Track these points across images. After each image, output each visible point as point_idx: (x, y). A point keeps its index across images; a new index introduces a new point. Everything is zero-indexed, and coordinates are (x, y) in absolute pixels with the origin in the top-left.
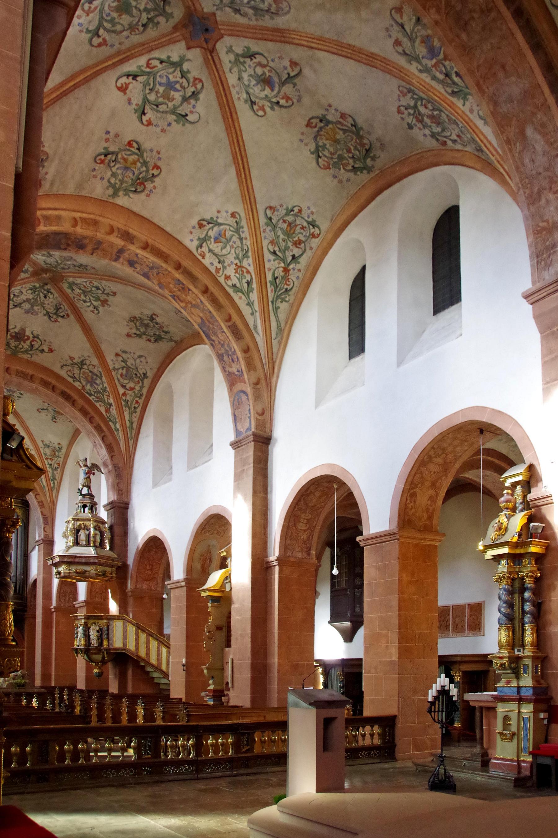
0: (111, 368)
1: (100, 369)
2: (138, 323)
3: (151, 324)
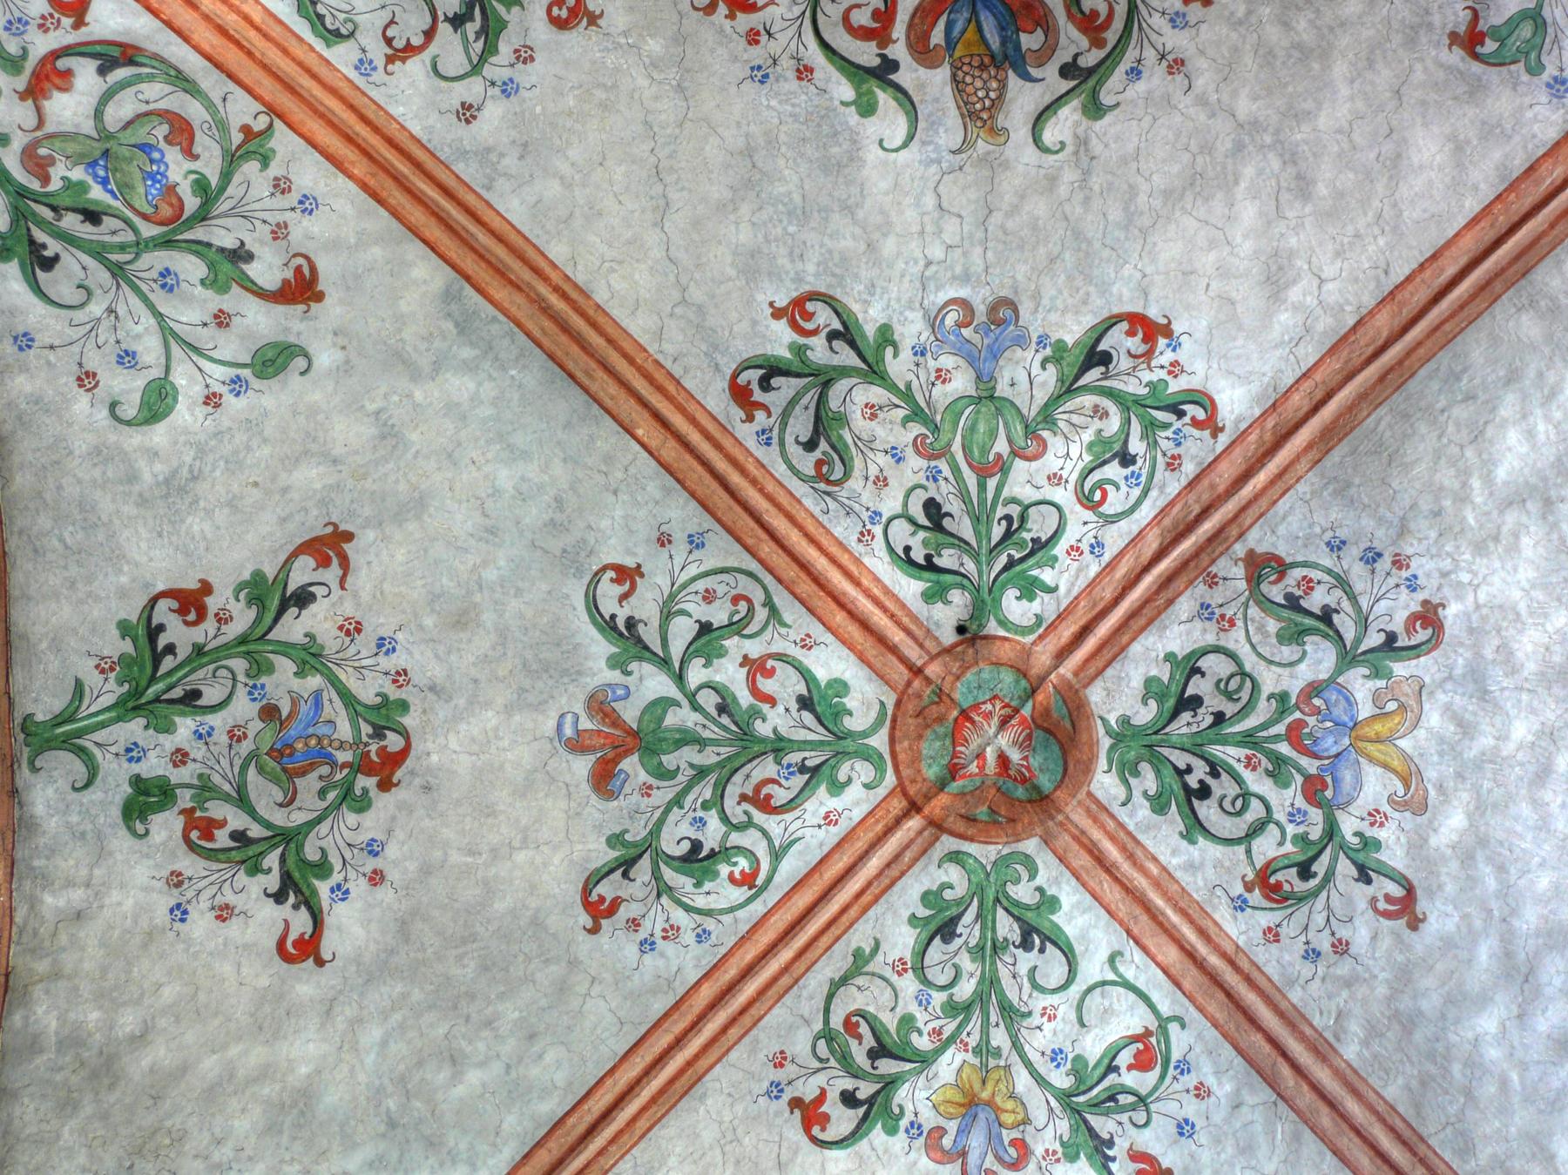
0: (283, 141)
1: (342, 57)
2: (344, 730)
3: (264, 794)
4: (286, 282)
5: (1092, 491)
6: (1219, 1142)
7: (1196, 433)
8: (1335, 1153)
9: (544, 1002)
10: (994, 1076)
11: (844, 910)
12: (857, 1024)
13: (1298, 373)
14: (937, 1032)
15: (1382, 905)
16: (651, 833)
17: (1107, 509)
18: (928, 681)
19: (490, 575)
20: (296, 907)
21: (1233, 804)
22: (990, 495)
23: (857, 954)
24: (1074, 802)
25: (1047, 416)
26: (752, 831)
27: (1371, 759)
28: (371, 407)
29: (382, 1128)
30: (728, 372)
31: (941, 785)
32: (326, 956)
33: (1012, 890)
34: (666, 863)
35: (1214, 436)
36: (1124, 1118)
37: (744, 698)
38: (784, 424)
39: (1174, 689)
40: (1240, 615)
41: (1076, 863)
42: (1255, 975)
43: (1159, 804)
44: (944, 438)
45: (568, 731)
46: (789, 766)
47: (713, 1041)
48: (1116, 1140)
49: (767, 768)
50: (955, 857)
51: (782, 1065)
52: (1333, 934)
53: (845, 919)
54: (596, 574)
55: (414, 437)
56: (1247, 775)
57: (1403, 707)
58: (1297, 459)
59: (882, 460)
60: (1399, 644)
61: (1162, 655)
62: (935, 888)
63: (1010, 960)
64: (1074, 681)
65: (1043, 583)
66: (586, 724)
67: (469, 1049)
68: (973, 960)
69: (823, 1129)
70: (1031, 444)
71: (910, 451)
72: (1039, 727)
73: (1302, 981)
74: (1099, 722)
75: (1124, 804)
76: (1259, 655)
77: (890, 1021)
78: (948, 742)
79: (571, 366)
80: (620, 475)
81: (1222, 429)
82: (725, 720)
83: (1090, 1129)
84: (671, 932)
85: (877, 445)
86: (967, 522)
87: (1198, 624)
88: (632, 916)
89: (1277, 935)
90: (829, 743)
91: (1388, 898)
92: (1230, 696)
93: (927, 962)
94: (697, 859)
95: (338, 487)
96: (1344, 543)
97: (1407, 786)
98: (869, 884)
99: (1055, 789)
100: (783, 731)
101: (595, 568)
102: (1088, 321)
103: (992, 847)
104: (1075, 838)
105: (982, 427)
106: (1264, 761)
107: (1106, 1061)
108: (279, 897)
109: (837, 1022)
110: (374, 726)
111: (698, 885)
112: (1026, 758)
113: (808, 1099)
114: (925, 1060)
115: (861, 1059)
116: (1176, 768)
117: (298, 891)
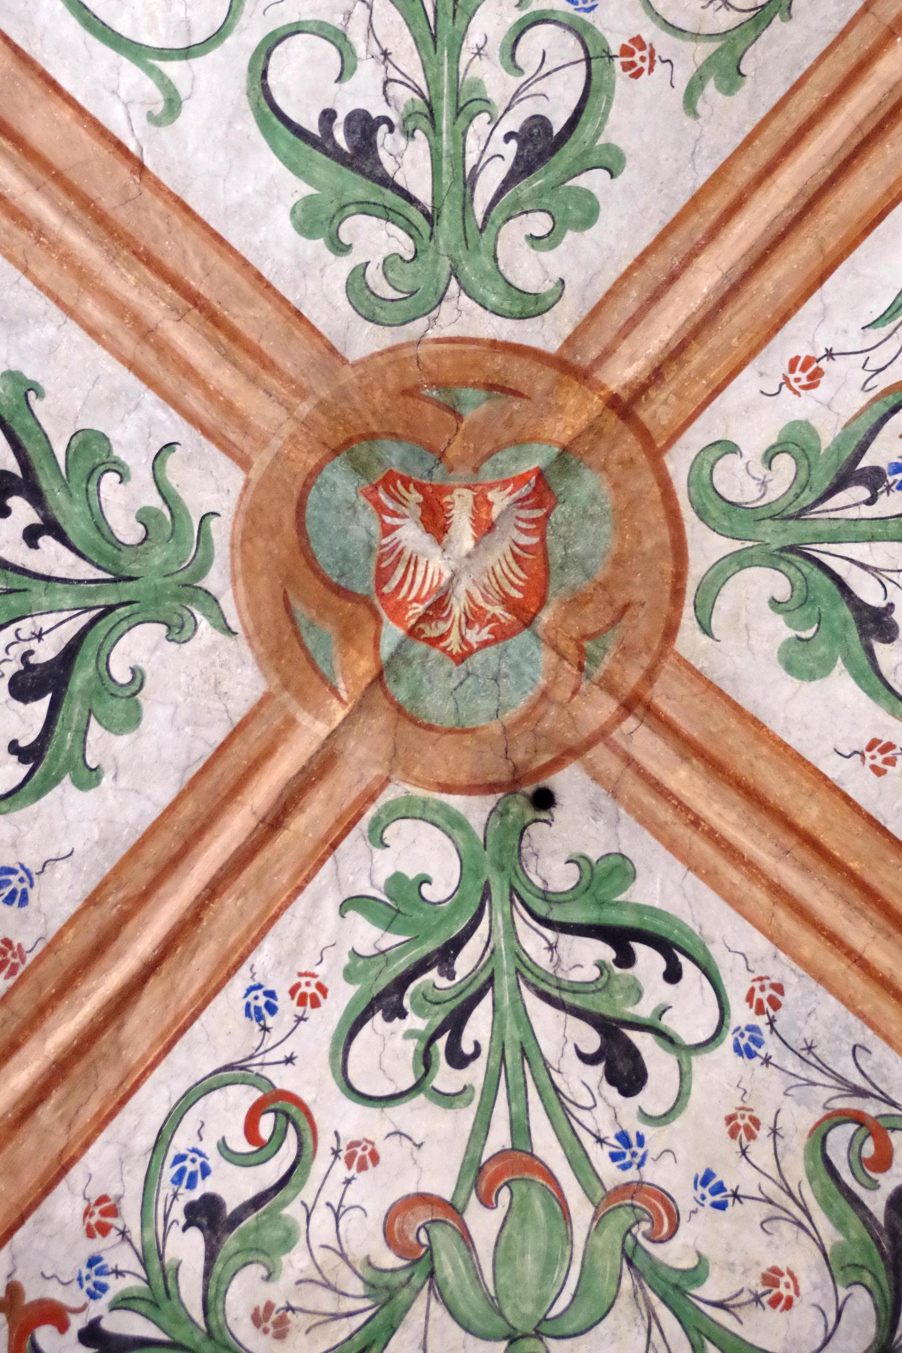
5: (279, 1135)
7: (56, 1293)
11: (768, 171)
18: (608, 686)
22: (501, 1109)
24: (276, 443)
33: (403, 244)
39: (73, 709)
41: (265, 310)
44: (610, 1238)
53: (763, 152)
61: (106, 781)
62: (570, 235)
64: (293, 707)
65: (374, 919)
68: (478, 84)
71: (685, 1198)
72: (365, 601)
74: (234, 623)
75: (169, 446)
78: (557, 553)
85: (758, 1211)
87: (33, 862)
90: (819, 538)
98: (713, 234)
99: (319, 468)
103: (450, 331)
104: (268, 365)
105: (530, 1266)
112: (388, 530)
116: (61, 537)
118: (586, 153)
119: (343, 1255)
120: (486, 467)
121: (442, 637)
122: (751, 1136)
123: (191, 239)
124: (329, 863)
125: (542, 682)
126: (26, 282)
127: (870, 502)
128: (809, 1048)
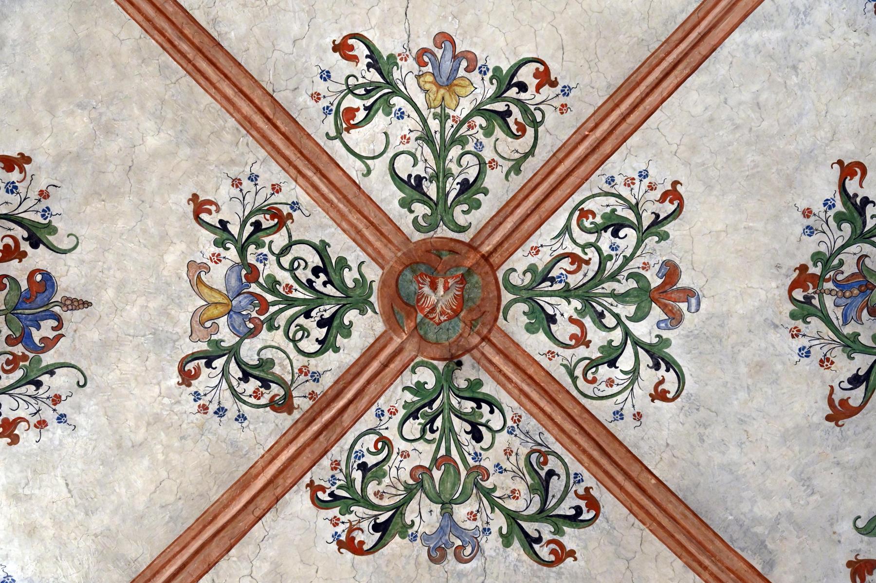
2: (829, 301)
4: (871, 573)
5: (383, 448)
6: (306, 68)
7: (322, 483)
8: (240, 64)
9: (705, 140)
10: (437, 103)
11: (527, 197)
12: (518, 130)
13: (263, 519)
14: (470, 127)
15: (213, 208)
16: (643, 241)
17: (374, 437)
18: (478, 333)
19: (743, 395)
20: (856, 195)
21: (299, 265)
22: (443, 444)
23: (518, 171)
24: (391, 263)
25: (410, 492)
26: (582, 242)
27: (219, 292)
28: (816, 497)
29: (801, 66)
30: (600, 518)
31: (470, 271)
32: (836, 166)
33: (428, 211)
34: (633, 223)
35: (312, 482)
36: (361, 81)
37: (588, 321)
38: (567, 486)
39: (334, 331)
40: (296, 376)
41: (390, 226)
42: (286, 165)
43: (342, 263)
45: (693, 301)
46: (560, 282)
47: (603, 120)
48: (366, 68)
49: (574, 280)
50: (462, 229)
51: (562, 105)
52: (241, 190)
53: (526, 192)
54: (679, 396)
55: (790, 479)
56: (291, 282)
57: (202, 324)
58: (264, 469)
59: (506, 465)
60: (204, 361)
61: (341, 351)
62: (473, 211)
63: (428, 170)
64: (392, 334)
65: (412, 393)
66: (683, 306)
67: (750, 112)
68: (450, 169)
69: (537, 69)
70: (420, 474)
71: (491, 470)
72: (413, 307)
73: (259, 163)
74: (377, 311)
75: (363, 262)
76: (285, 352)
77: (498, 132)
78: (466, 296)
79: (696, 521)
80: (665, 455)
81: (307, 486)
82: (599, 309)
83: (381, 74)
84: (629, 183)
86: (457, 429)
87: (321, 370)
88: (653, 192)
89: (273, 189)
91: (209, 212)
92: (301, 327)
93: (477, 168)
94: (615, 225)
95: (836, 448)
96: (236, 420)
97: (199, 277)
98: (512, 213)
100: (564, 302)
101: (679, 399)
102: (385, 550)
103: (440, 235)
105: (449, 485)
106: (281, 290)
107: (372, 113)
108: (866, 201)
109: (530, 131)
110: (811, 304)
111: (614, 211)
112: (420, 288)
113: (547, 87)
114: (478, 111)
115: (515, 109)
116: (333, 285)
117: (855, 205)
118: (480, 188)
119: (399, 480)
120: (448, 272)
121: (434, 318)
122: (510, 455)
123: (371, 207)
124: (400, 377)
125: (460, 331)
126: (327, 217)
127: (551, 286)
128: (528, 433)
